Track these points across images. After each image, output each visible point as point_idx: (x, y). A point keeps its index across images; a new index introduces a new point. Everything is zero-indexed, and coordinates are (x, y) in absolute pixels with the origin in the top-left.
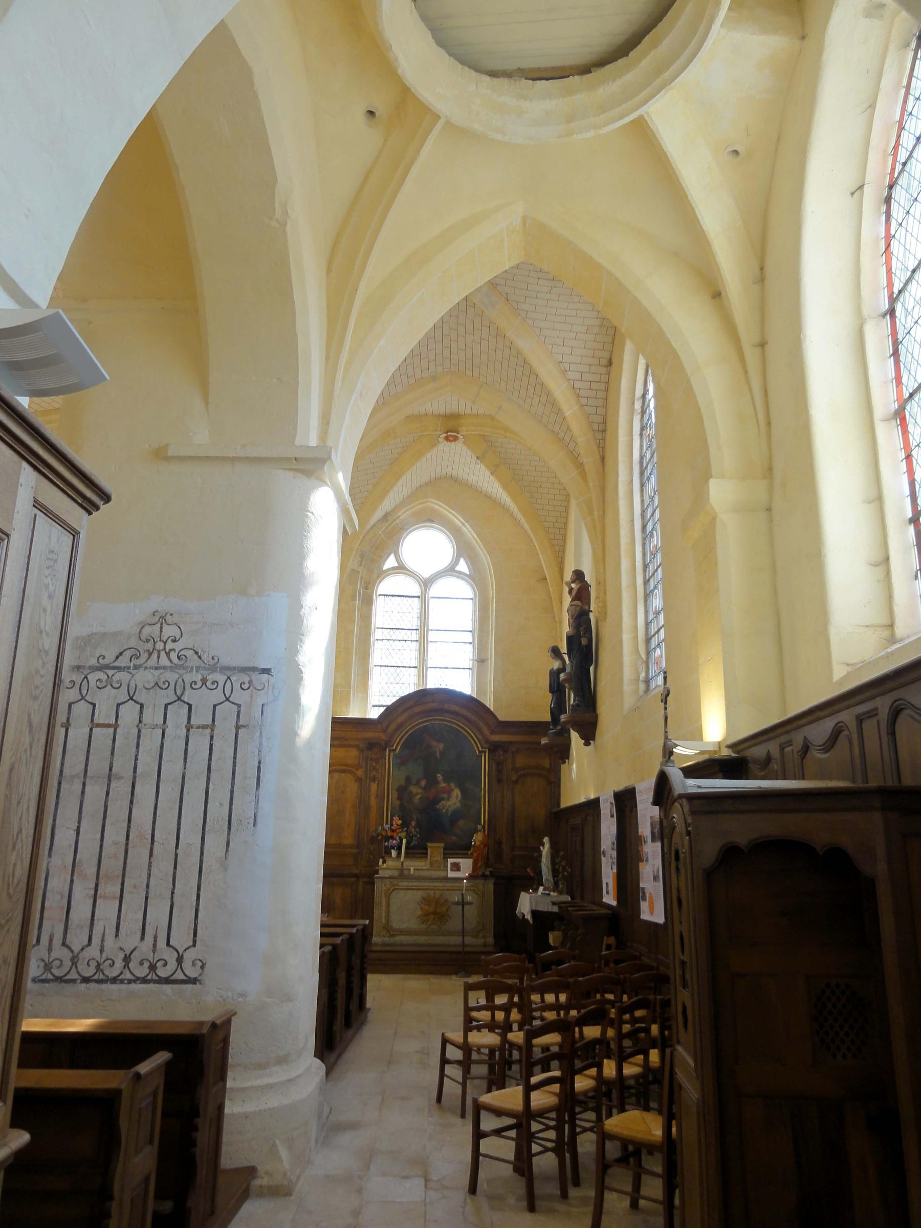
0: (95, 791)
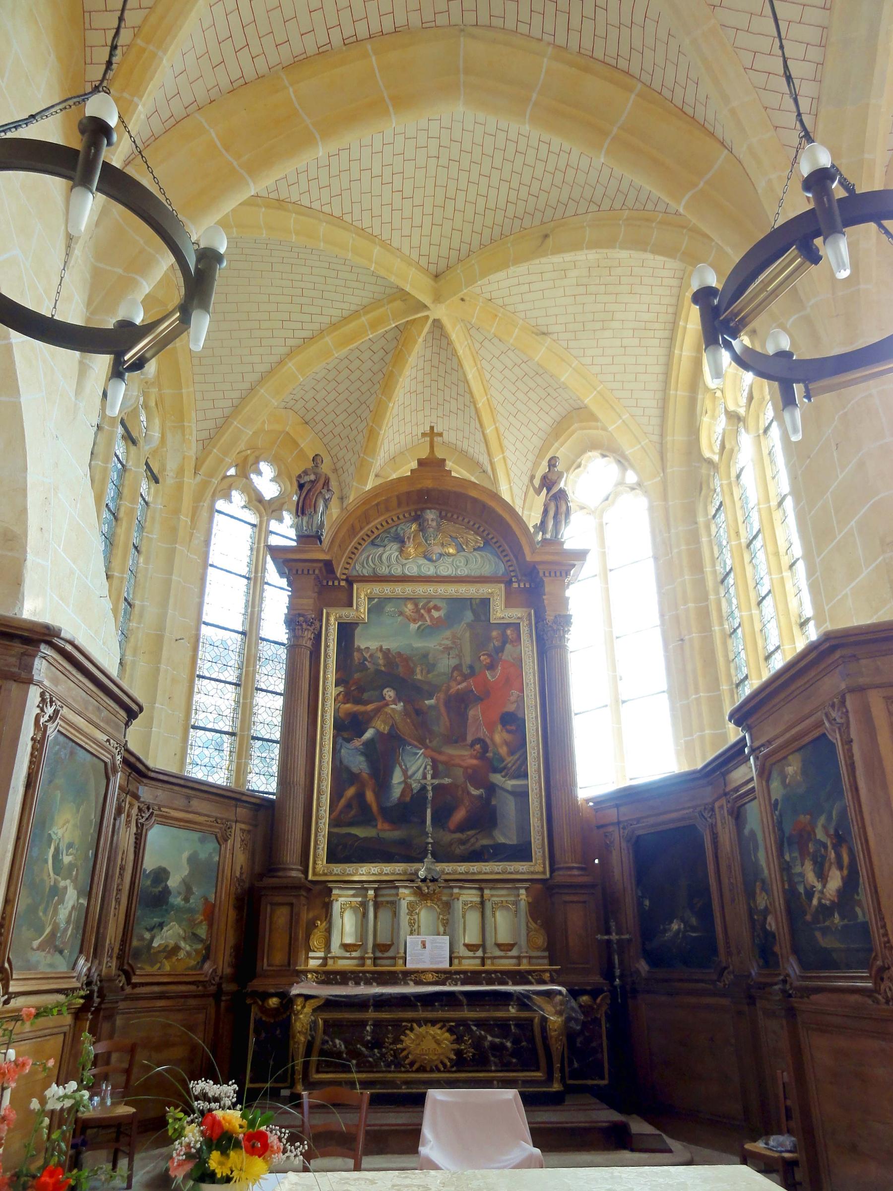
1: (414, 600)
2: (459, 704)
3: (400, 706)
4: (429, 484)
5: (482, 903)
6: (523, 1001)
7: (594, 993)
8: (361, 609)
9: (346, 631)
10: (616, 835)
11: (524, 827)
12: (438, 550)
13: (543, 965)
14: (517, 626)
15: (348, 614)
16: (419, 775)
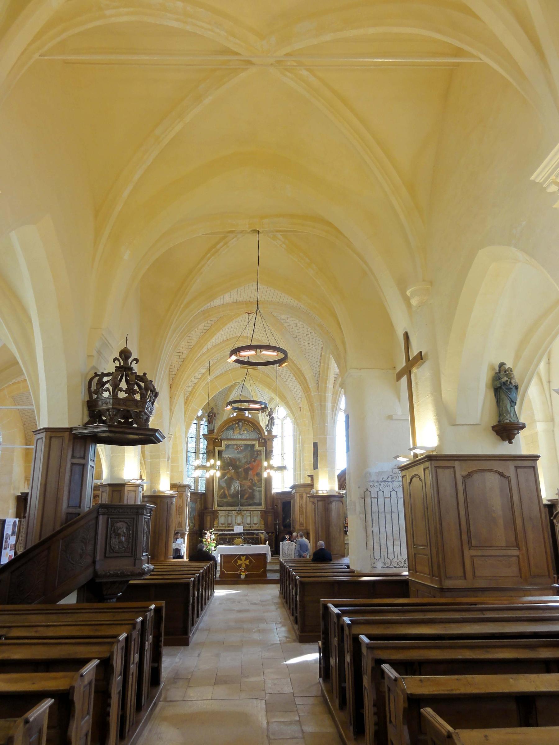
0: (388, 516)
1: (237, 445)
2: (247, 471)
3: (233, 471)
4: (240, 417)
5: (251, 516)
6: (257, 534)
7: (272, 533)
8: (224, 448)
9: (220, 453)
10: (280, 502)
11: (260, 499)
12: (242, 432)
13: (263, 528)
14: (261, 451)
15: (221, 449)
16: (237, 488)
